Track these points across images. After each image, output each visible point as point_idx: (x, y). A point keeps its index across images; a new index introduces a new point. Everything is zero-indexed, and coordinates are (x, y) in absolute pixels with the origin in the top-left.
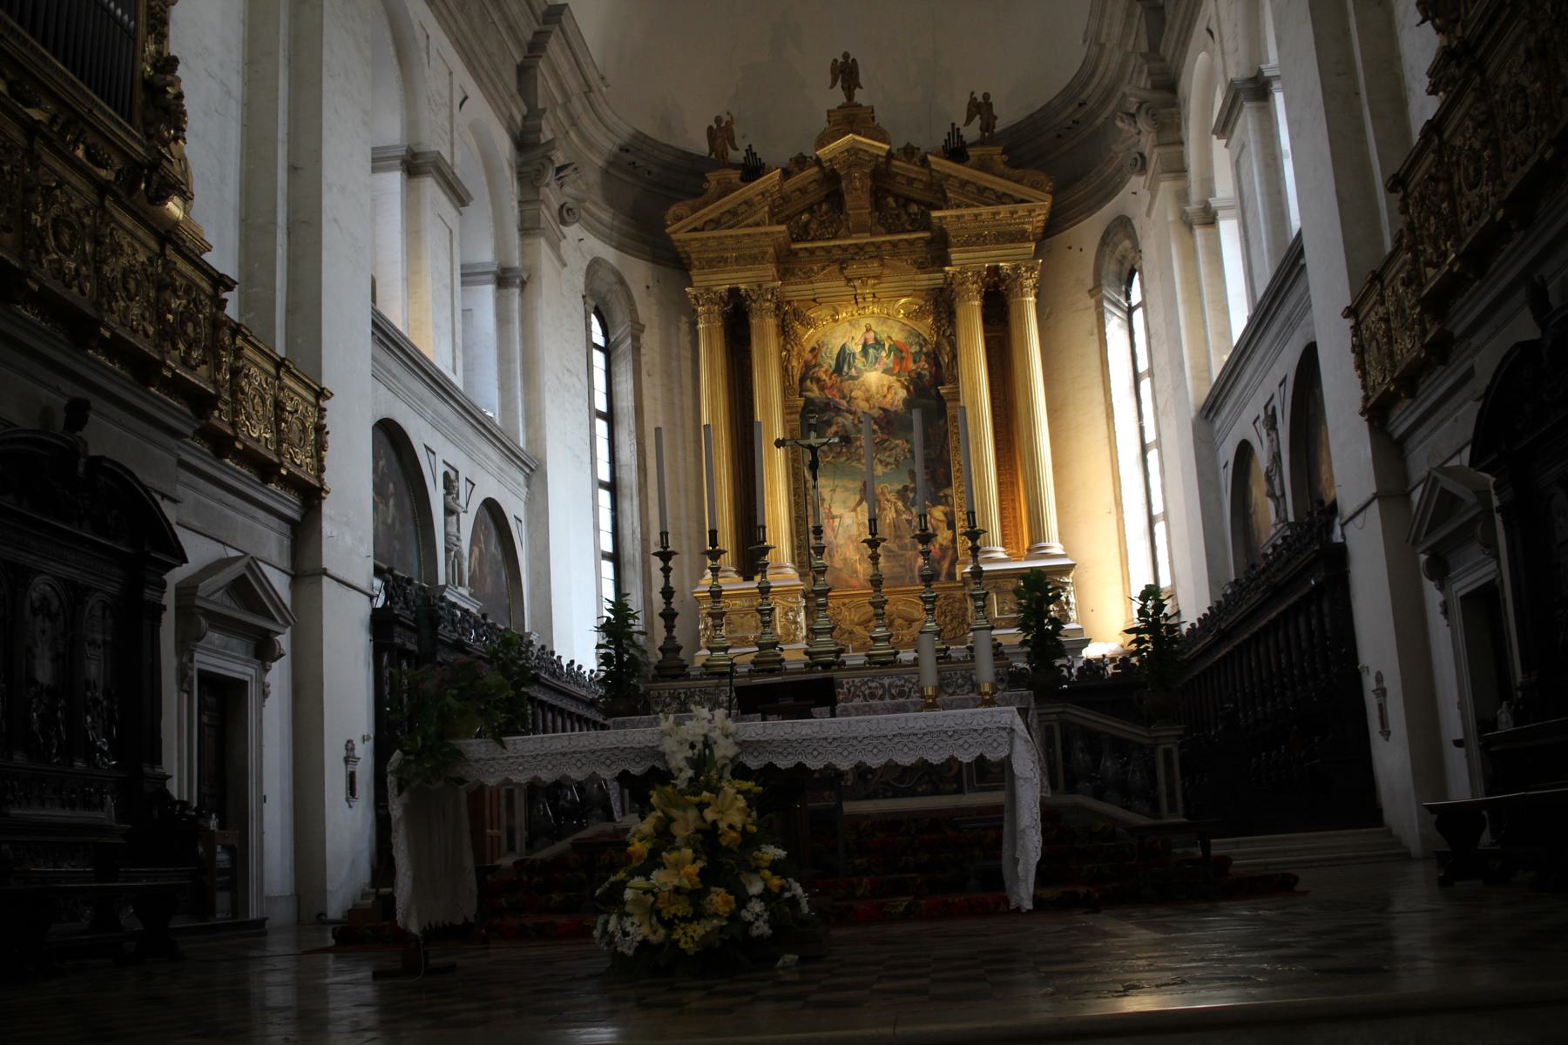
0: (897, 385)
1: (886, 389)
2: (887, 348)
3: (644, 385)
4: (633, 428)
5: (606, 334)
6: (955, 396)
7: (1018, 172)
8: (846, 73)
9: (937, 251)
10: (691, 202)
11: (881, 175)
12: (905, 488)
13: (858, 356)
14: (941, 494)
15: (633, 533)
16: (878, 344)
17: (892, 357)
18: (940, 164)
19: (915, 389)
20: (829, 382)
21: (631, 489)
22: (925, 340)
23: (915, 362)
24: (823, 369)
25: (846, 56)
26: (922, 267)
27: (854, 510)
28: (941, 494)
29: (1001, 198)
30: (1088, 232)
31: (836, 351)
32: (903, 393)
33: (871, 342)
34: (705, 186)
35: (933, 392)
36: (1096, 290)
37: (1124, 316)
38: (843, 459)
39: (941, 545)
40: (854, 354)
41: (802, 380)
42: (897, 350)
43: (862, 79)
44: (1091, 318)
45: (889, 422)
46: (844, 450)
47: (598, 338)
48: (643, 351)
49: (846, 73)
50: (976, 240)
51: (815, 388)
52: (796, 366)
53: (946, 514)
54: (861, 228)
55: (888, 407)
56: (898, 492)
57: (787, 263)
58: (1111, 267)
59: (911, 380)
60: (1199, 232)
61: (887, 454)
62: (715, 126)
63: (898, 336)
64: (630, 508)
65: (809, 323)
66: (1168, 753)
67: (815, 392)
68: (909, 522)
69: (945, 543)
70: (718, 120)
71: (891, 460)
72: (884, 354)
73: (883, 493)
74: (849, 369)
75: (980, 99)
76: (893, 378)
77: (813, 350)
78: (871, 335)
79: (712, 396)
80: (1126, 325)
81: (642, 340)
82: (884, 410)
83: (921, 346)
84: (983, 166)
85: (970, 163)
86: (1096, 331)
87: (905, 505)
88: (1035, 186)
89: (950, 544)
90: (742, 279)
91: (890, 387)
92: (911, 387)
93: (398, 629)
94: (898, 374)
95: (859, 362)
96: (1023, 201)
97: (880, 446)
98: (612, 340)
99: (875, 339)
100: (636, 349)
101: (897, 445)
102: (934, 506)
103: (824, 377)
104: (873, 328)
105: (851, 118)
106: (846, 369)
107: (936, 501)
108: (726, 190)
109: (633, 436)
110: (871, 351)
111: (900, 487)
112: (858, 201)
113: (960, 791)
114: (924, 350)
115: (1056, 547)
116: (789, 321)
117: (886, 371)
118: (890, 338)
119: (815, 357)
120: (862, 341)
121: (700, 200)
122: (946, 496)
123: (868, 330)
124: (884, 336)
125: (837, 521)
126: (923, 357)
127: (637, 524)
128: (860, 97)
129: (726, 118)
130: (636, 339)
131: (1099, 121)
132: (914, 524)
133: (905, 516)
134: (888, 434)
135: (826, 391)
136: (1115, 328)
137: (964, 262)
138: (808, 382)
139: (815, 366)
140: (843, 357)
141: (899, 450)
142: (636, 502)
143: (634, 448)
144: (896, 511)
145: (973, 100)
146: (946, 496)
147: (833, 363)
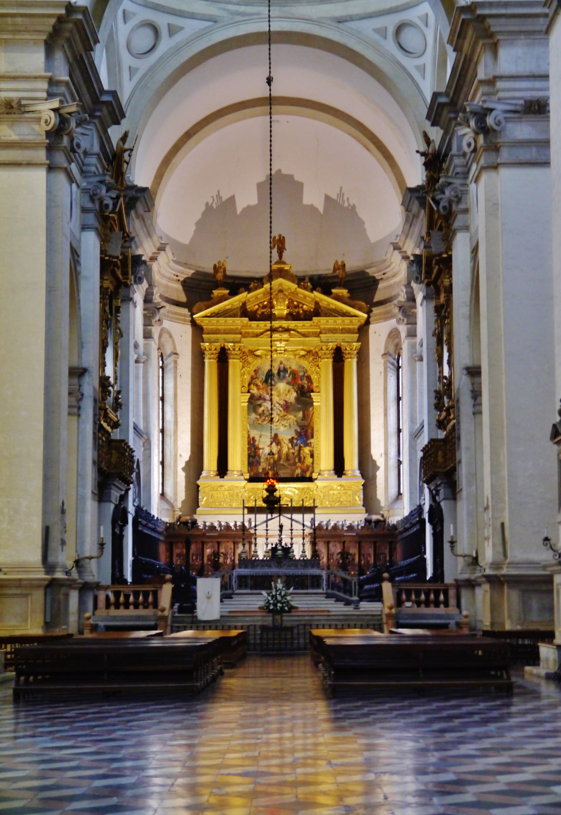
0: (292, 390)
1: (287, 392)
2: (289, 372)
3: (178, 383)
4: (173, 404)
5: (163, 363)
7: (352, 302)
10: (205, 303)
12: (293, 438)
13: (276, 375)
14: (309, 442)
15: (171, 452)
16: (285, 370)
17: (291, 377)
18: (318, 295)
19: (300, 392)
20: (261, 386)
21: (171, 432)
22: (306, 370)
23: (301, 380)
24: (260, 380)
25: (280, 236)
27: (269, 446)
28: (309, 442)
31: (266, 372)
32: (295, 394)
33: (282, 369)
34: (212, 296)
35: (308, 394)
37: (395, 370)
38: (266, 422)
39: (307, 465)
40: (274, 374)
41: (249, 384)
43: (287, 246)
44: (382, 368)
46: (267, 418)
47: (161, 365)
48: (178, 367)
51: (255, 388)
53: (310, 451)
54: (281, 318)
55: (287, 400)
56: (289, 440)
59: (299, 389)
60: (418, 363)
61: (286, 421)
62: (217, 265)
64: (168, 440)
66: (355, 583)
67: (254, 391)
68: (293, 453)
69: (309, 464)
70: (219, 262)
71: (287, 425)
72: (287, 375)
73: (283, 440)
74: (271, 381)
75: (340, 263)
76: (290, 387)
77: (255, 371)
78: (282, 366)
79: (210, 393)
80: (396, 373)
81: (178, 362)
82: (286, 401)
83: (304, 373)
84: (338, 298)
85: (333, 296)
86: (383, 374)
87: (292, 445)
89: (311, 465)
91: (289, 391)
92: (299, 392)
93: (140, 525)
94: (293, 385)
95: (276, 378)
96: (355, 316)
97: (283, 418)
98: (165, 362)
99: (284, 368)
100: (176, 367)
101: (290, 419)
102: (305, 447)
103: (260, 384)
104: (284, 362)
106: (269, 381)
107: (307, 445)
109: (173, 408)
110: (282, 373)
111: (290, 437)
113: (307, 589)
114: (306, 375)
117: (288, 383)
118: (290, 368)
119: (256, 374)
120: (278, 368)
121: (209, 303)
122: (311, 443)
123: (281, 363)
124: (288, 367)
125: (261, 451)
126: (305, 378)
127: (172, 448)
128: (285, 254)
129: (222, 262)
130: (176, 362)
131: (392, 281)
132: (296, 454)
133: (292, 451)
134: (287, 412)
135: (260, 391)
138: (252, 386)
139: (255, 378)
141: (291, 420)
142: (172, 438)
143: (173, 413)
144: (288, 448)
145: (337, 262)
146: (311, 443)
147: (264, 378)
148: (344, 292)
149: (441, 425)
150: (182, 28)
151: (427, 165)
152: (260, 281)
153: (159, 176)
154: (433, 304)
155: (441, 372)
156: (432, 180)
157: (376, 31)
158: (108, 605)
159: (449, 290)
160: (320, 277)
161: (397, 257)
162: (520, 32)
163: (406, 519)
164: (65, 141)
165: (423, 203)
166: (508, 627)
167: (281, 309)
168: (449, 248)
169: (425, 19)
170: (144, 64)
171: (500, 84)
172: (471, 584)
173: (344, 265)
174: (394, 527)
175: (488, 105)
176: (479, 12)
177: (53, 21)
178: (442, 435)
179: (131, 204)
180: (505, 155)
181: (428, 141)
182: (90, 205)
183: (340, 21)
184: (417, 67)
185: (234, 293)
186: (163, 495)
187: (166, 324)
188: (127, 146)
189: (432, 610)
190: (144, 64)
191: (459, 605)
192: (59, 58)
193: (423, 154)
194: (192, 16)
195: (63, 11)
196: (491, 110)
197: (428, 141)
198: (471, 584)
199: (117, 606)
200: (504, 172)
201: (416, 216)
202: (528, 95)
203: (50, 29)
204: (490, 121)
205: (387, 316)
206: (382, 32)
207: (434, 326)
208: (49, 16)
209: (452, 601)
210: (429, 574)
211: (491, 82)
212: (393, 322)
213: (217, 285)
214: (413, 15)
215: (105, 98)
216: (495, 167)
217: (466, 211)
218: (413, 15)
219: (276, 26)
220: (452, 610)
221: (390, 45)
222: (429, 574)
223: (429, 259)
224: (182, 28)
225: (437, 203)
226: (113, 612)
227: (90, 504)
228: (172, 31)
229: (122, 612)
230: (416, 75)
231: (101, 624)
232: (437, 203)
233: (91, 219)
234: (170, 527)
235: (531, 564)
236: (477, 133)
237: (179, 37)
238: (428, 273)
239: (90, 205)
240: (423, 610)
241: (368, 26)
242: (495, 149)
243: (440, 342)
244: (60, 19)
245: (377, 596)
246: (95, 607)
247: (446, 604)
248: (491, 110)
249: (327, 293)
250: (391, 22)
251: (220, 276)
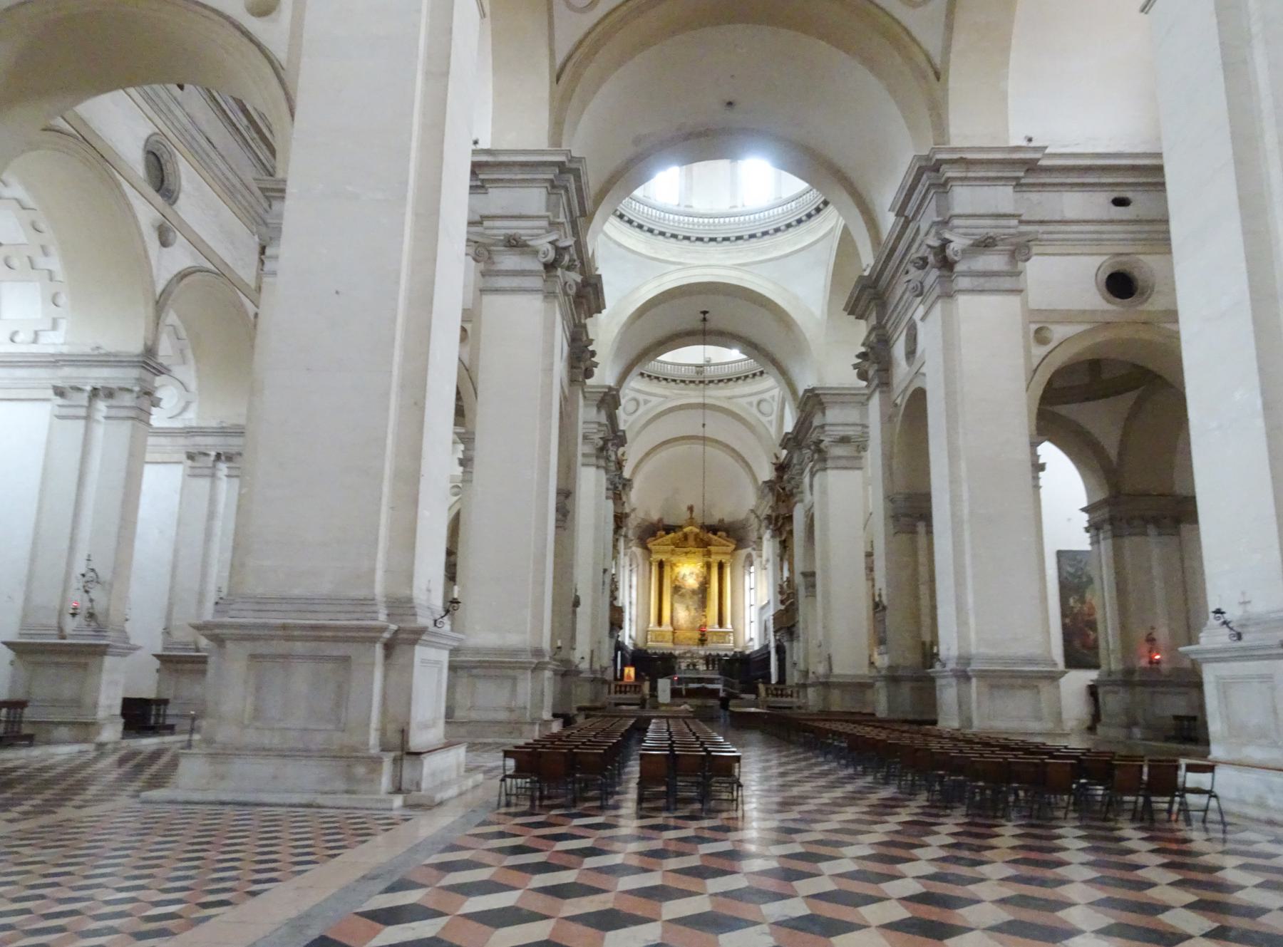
6: (709, 587)
8: (691, 509)
9: (709, 554)
11: (696, 535)
18: (710, 535)
26: (704, 555)
29: (724, 545)
30: (743, 553)
36: (744, 567)
42: (697, 575)
45: (694, 592)
49: (691, 509)
50: (717, 553)
52: (674, 577)
54: (691, 546)
57: (673, 552)
58: (748, 563)
63: (698, 572)
65: (678, 567)
67: (677, 583)
84: (720, 537)
88: (732, 542)
90: (664, 558)
105: (691, 522)
108: (662, 537)
112: (691, 539)
115: (728, 626)
116: (673, 565)
136: (747, 577)
137: (715, 559)
140: (684, 576)
148: (724, 534)
149: (782, 602)
150: (650, 401)
151: (777, 469)
152: (681, 527)
153: (634, 472)
154: (778, 539)
155: (782, 575)
156: (780, 478)
157: (747, 403)
158: (616, 692)
159: (791, 532)
160: (711, 526)
161: (753, 516)
162: (836, 402)
163: (757, 651)
164: (605, 453)
165: (772, 489)
166: (835, 708)
167: (691, 539)
168: (791, 510)
169: (773, 397)
170: (631, 419)
171: (827, 428)
172: (804, 686)
173: (723, 520)
174: (749, 655)
175: (821, 438)
176: (817, 392)
177: (602, 395)
178: (783, 607)
179: (624, 486)
180: (830, 463)
181: (777, 458)
182: (610, 487)
183: (730, 398)
184: (769, 421)
185: (668, 533)
186: (630, 637)
187: (634, 549)
188: (625, 458)
189: (784, 699)
190: (631, 419)
191: (798, 697)
192: (603, 413)
193: (774, 464)
194: (655, 395)
195: (607, 390)
196: (822, 441)
197: (777, 458)
198: (804, 686)
199: (621, 692)
200: (829, 472)
201: (765, 496)
202: (842, 434)
203: (599, 398)
204: (822, 446)
205: (746, 547)
206: (751, 404)
207: (778, 551)
208: (600, 392)
209: (795, 695)
210: (774, 680)
211: (822, 427)
212: (749, 550)
213: (659, 530)
214: (766, 396)
215: (620, 434)
216: (825, 469)
217: (802, 492)
218: (766, 396)
219: (708, 401)
220: (794, 700)
221: (754, 410)
222: (774, 680)
223: (777, 518)
224: (650, 401)
225: (784, 489)
226: (618, 696)
227: (607, 639)
228: (646, 402)
229: (623, 696)
230: (768, 425)
231: (613, 701)
232: (784, 489)
233: (610, 493)
234: (633, 652)
235: (845, 676)
236: (814, 452)
237: (649, 405)
238: (776, 524)
239: (610, 487)
240: (779, 699)
241: (743, 401)
242: (824, 460)
243: (782, 560)
244: (605, 394)
245: (755, 691)
246: (609, 692)
247: (791, 696)
248: (822, 441)
249: (715, 533)
250: (755, 399)
251: (661, 525)
